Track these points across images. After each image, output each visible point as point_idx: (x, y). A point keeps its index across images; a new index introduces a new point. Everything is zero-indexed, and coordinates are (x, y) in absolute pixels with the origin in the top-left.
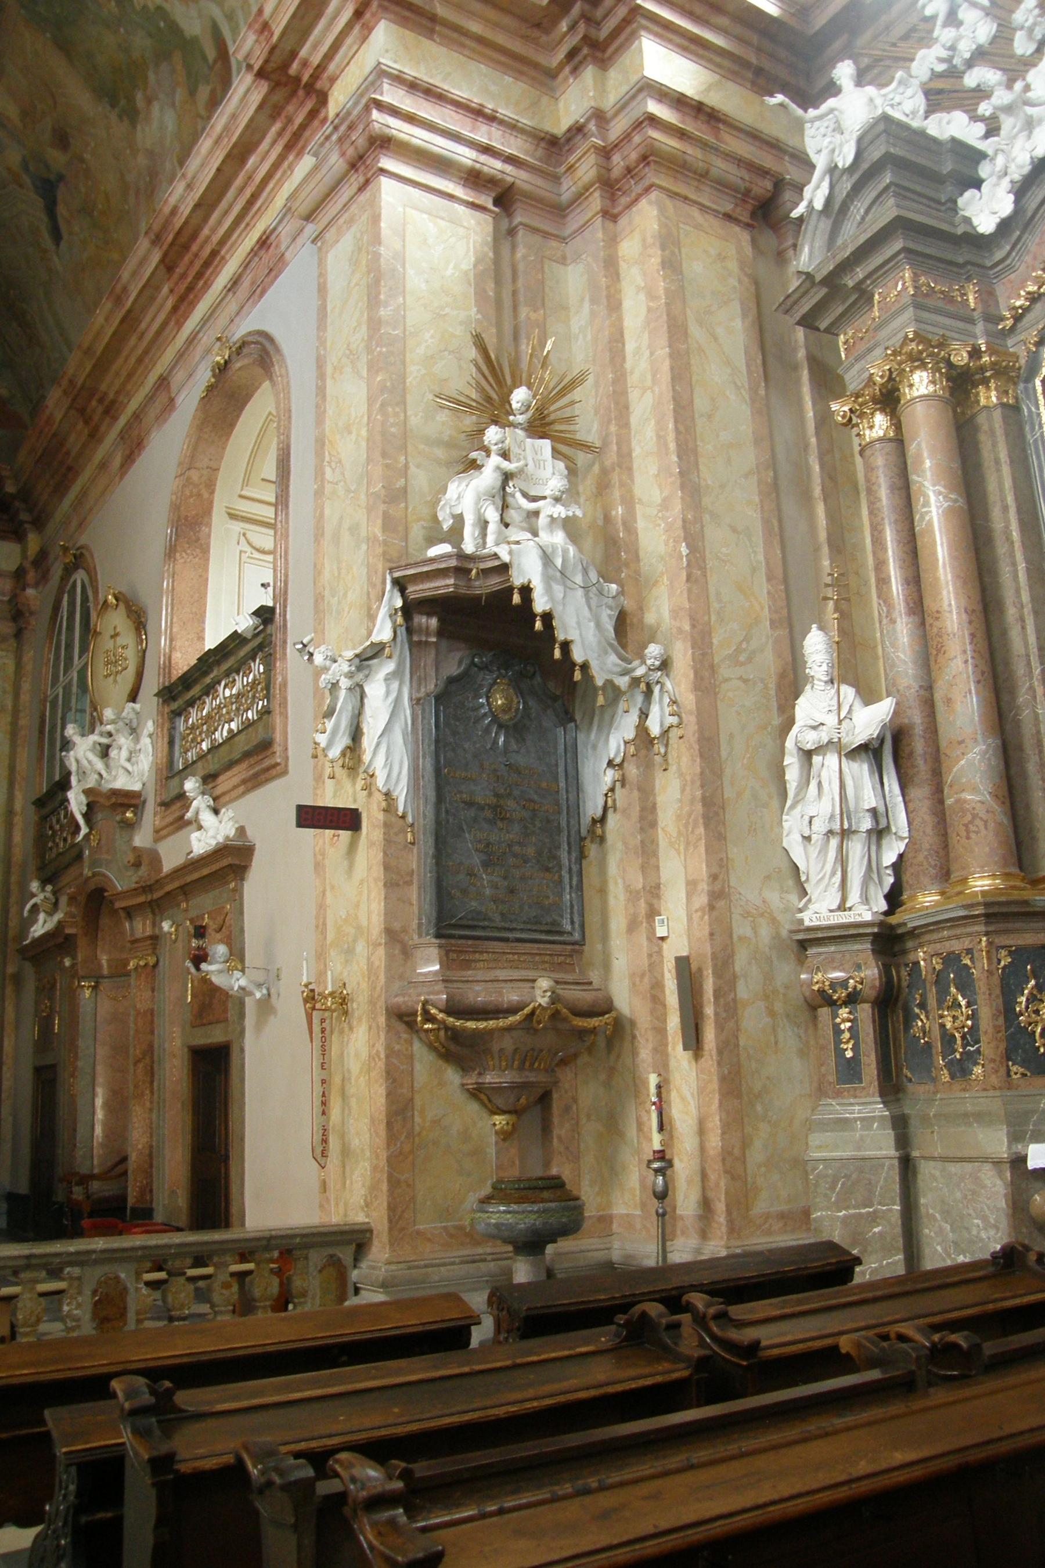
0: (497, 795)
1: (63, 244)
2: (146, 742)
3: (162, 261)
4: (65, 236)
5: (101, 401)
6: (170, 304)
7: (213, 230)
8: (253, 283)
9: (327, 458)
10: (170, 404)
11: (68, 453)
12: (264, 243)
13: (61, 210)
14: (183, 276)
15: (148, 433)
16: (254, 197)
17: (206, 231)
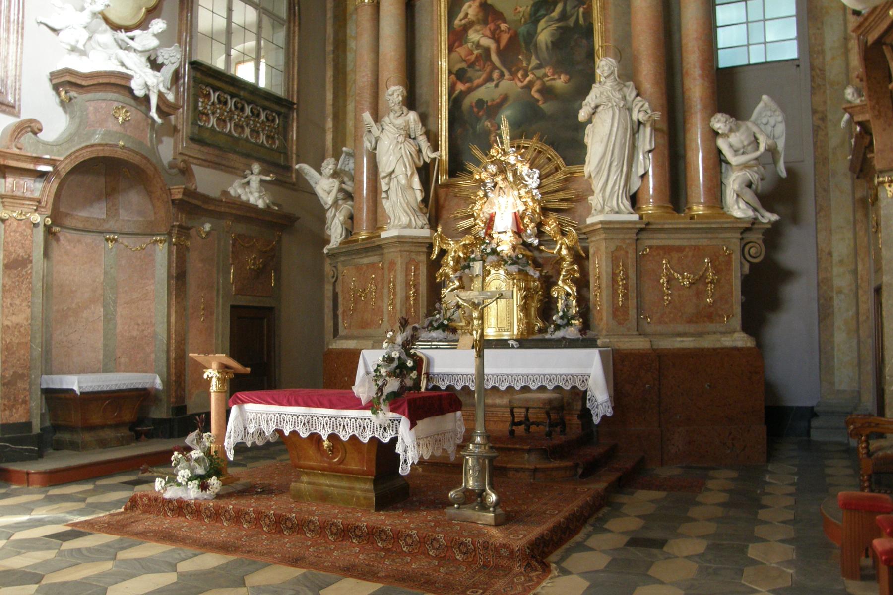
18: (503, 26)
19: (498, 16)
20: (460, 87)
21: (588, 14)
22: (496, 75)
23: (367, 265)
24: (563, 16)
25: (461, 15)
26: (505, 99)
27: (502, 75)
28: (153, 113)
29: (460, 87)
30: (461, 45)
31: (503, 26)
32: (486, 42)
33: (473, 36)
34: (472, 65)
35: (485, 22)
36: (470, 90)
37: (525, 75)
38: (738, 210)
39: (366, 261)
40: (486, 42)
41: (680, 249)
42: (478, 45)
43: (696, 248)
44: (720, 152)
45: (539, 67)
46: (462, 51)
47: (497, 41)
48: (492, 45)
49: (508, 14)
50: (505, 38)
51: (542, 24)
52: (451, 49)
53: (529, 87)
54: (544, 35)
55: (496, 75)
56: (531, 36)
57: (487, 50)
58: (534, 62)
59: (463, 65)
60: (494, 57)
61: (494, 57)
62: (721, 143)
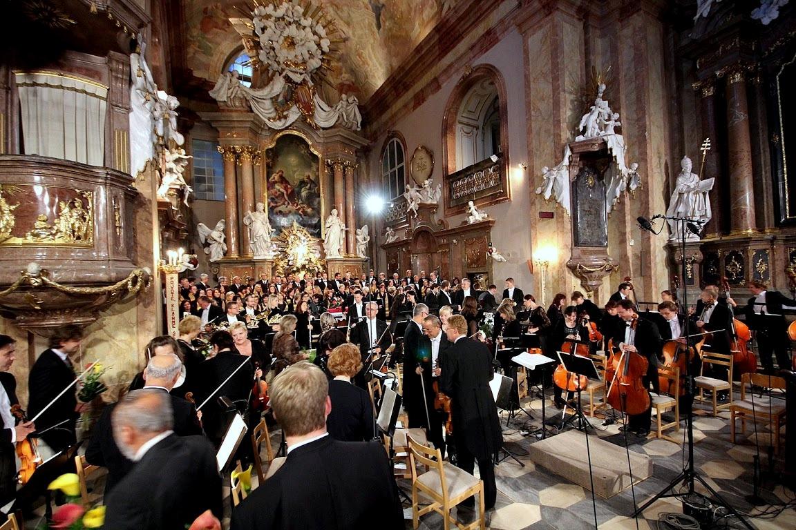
0: (590, 208)
1: (381, 30)
2: (438, 190)
3: (439, 39)
4: (382, 27)
5: (403, 85)
6: (438, 53)
7: (461, 27)
8: (481, 47)
9: (532, 108)
10: (439, 87)
11: (386, 101)
12: (488, 33)
13: (382, 18)
14: (446, 43)
15: (428, 96)
16: (481, 15)
17: (458, 27)
18: (289, 186)
19: (287, 182)
20: (272, 204)
21: (318, 190)
22: (286, 203)
23: (242, 268)
24: (310, 188)
25: (272, 177)
26: (290, 212)
27: (289, 204)
28: (185, 202)
29: (272, 204)
30: (272, 189)
31: (289, 186)
32: (282, 190)
33: (277, 187)
34: (277, 197)
35: (282, 183)
36: (276, 207)
37: (297, 206)
38: (362, 256)
39: (241, 266)
40: (282, 190)
41: (350, 266)
42: (279, 191)
43: (354, 266)
44: (356, 239)
45: (302, 204)
46: (272, 191)
47: (287, 191)
48: (285, 193)
49: (291, 183)
50: (290, 191)
51: (303, 189)
52: (268, 189)
53: (299, 209)
54: (304, 194)
55: (286, 203)
56: (299, 193)
57: (283, 193)
58: (300, 202)
59: (273, 197)
60: (285, 196)
61: (285, 196)
62: (358, 237)
